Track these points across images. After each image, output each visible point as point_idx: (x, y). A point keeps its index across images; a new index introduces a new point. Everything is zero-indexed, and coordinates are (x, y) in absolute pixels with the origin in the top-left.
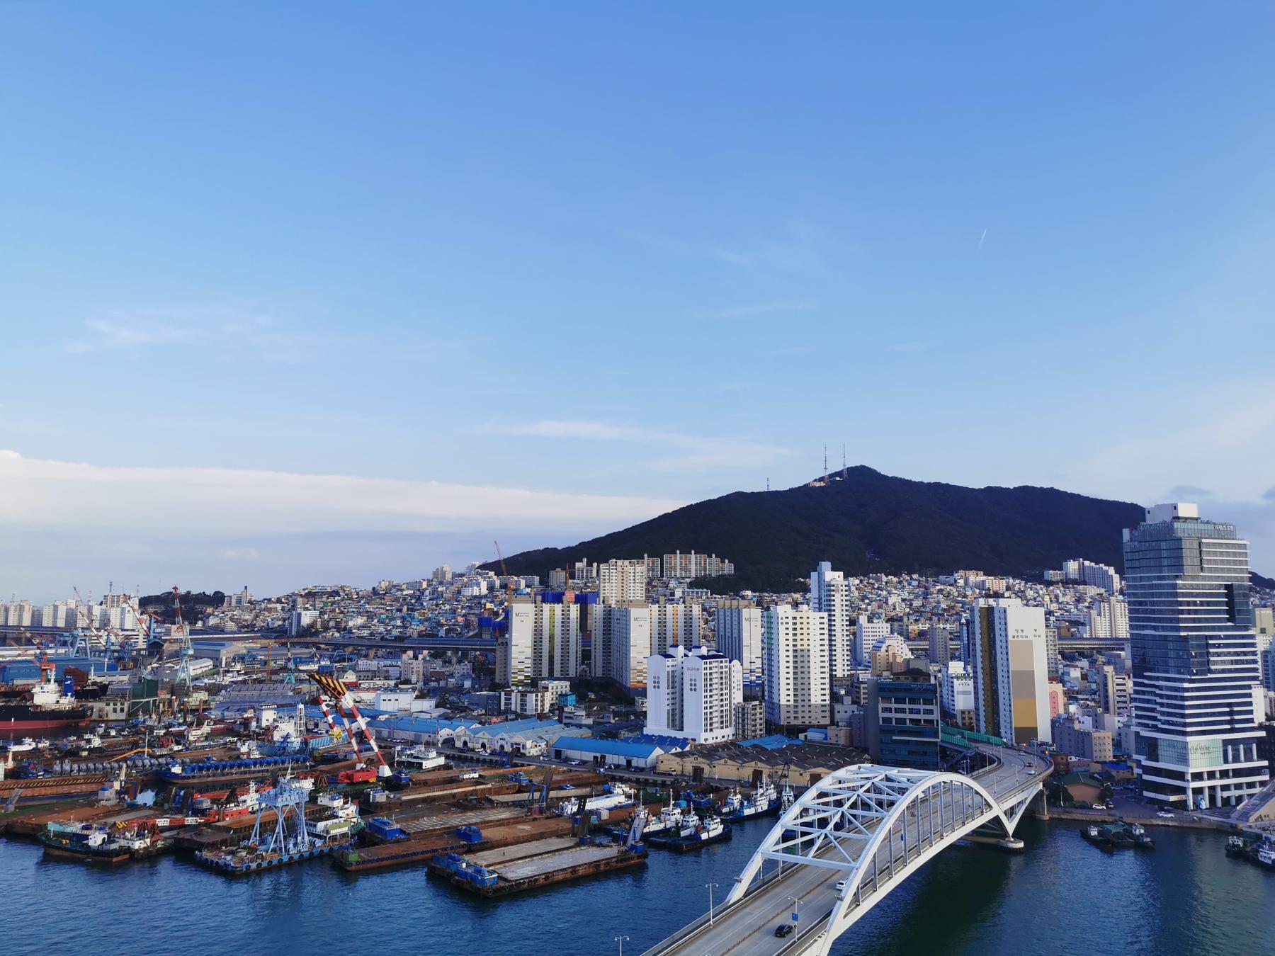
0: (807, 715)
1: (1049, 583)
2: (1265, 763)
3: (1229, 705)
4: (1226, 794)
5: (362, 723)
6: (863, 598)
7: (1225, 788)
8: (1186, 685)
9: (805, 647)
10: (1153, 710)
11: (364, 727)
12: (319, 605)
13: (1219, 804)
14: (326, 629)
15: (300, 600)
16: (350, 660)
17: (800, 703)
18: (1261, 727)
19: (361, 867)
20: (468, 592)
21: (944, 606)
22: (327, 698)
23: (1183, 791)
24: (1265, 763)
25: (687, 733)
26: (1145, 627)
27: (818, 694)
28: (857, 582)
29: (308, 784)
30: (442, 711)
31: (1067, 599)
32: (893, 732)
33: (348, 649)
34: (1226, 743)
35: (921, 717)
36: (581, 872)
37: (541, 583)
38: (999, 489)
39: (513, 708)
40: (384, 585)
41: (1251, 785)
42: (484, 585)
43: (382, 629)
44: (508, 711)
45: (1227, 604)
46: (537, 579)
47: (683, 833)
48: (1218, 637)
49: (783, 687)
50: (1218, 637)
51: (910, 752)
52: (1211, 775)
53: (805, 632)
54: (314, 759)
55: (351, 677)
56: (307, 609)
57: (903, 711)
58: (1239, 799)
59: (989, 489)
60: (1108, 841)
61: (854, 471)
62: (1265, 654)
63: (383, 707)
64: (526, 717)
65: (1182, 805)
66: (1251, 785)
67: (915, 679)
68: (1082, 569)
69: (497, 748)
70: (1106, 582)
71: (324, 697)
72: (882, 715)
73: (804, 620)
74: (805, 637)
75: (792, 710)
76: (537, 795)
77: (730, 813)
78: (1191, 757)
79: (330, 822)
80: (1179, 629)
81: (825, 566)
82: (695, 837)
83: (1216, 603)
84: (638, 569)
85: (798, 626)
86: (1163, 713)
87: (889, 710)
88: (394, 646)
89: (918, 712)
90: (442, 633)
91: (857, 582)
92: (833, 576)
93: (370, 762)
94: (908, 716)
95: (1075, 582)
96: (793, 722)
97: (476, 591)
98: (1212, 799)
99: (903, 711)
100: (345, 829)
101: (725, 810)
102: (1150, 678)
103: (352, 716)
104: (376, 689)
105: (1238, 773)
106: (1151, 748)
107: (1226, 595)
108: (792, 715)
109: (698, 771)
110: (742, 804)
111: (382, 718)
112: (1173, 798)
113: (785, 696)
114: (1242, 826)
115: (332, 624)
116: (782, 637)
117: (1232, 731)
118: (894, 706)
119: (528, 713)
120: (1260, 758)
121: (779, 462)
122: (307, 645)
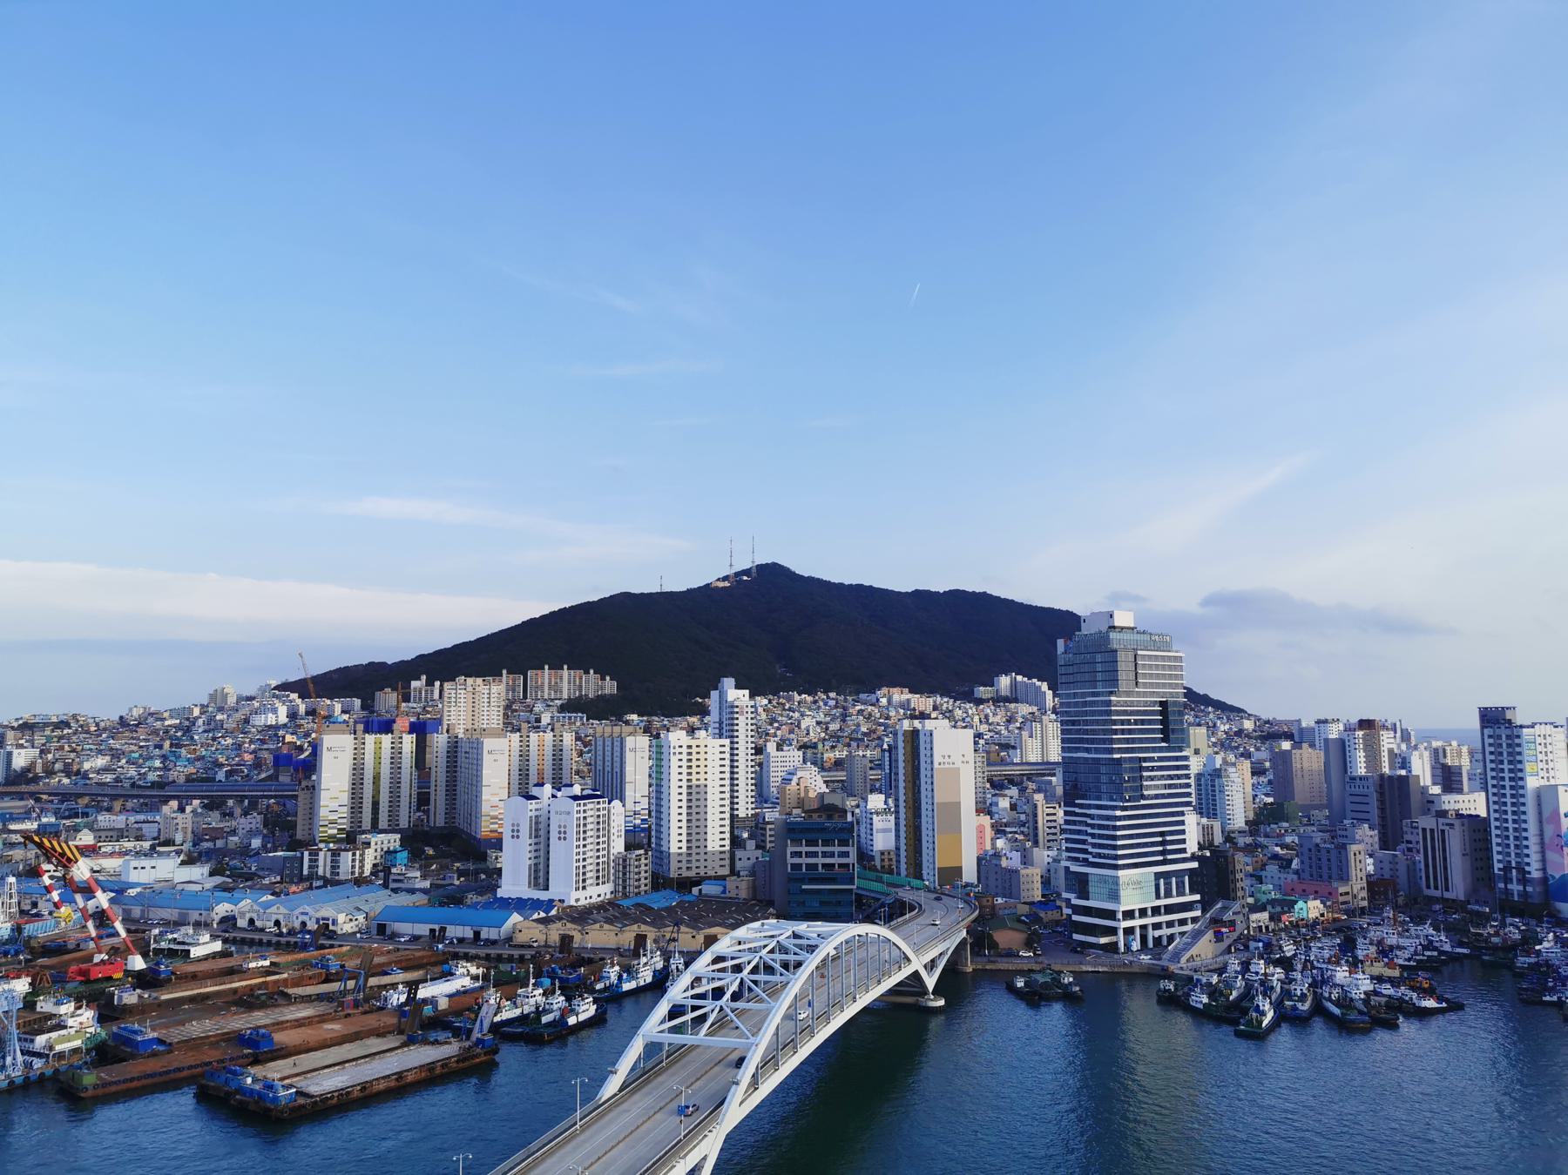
0: (702, 864)
1: (979, 702)
2: (1197, 897)
3: (1162, 834)
4: (1157, 933)
5: (102, 899)
6: (772, 721)
7: (1157, 926)
8: (1118, 813)
9: (702, 782)
10: (1084, 842)
11: (105, 905)
12: (39, 740)
13: (1151, 944)
14: (50, 772)
15: (10, 735)
16: (85, 815)
17: (694, 851)
18: (1193, 858)
19: (100, 1092)
20: (260, 720)
21: (864, 729)
22: (51, 867)
23: (1113, 931)
24: (1197, 897)
25: (553, 893)
26: (1077, 750)
27: (717, 839)
28: (765, 702)
29: (21, 986)
30: (218, 880)
31: (997, 719)
32: (803, 880)
33: (82, 800)
34: (1158, 876)
35: (836, 860)
36: (410, 1078)
37: (363, 708)
38: (928, 593)
39: (321, 872)
40: (135, 713)
41: (1183, 922)
42: (283, 712)
43: (132, 772)
44: (313, 876)
45: (1162, 722)
46: (357, 702)
47: (544, 1019)
48: (1151, 759)
49: (674, 831)
50: (1151, 759)
51: (822, 903)
52: (1143, 912)
53: (702, 763)
54: (32, 951)
55: (86, 838)
56: (22, 746)
57: (815, 855)
58: (1171, 938)
59: (917, 593)
60: (1034, 993)
62: (1199, 776)
63: (134, 877)
64: (339, 883)
65: (1113, 947)
66: (1183, 922)
67: (830, 817)
68: (1014, 684)
69: (297, 925)
70: (1038, 700)
71: (45, 867)
72: (790, 861)
73: (702, 750)
74: (702, 769)
75: (684, 858)
76: (351, 984)
77: (606, 989)
78: (1122, 893)
79: (54, 1035)
80: (1111, 751)
81: (728, 683)
82: (560, 1022)
83: (1150, 722)
84: (495, 689)
85: (694, 757)
86: (1094, 845)
87: (799, 854)
88: (150, 796)
89: (832, 855)
90: (221, 776)
91: (765, 702)
92: (737, 696)
93: (114, 951)
94: (820, 861)
95: (1007, 700)
96: (685, 874)
97: (271, 719)
98: (1144, 938)
99: (815, 855)
100: (77, 1043)
101: (599, 986)
102: (1081, 806)
103: (88, 892)
104: (122, 854)
105: (1170, 909)
106: (1080, 884)
107: (1161, 713)
108: (684, 865)
109: (566, 940)
110: (620, 978)
111: (132, 892)
112: (1103, 940)
113: (676, 842)
114: (1173, 968)
115: (58, 766)
116: (674, 770)
117: (1164, 862)
118: (804, 849)
119: (342, 877)
120: (1192, 891)
121: (676, 555)
122: (21, 796)
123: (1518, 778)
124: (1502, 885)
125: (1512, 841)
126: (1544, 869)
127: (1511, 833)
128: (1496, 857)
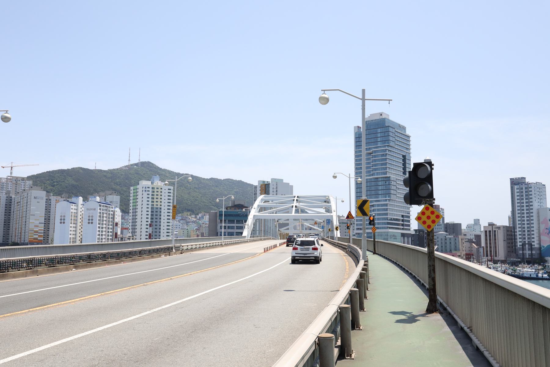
9: (159, 206)
53: (159, 197)
59: (211, 179)
61: (143, 164)
74: (159, 200)
99: (233, 228)
123: (529, 206)
124: (521, 252)
125: (526, 233)
126: (540, 244)
127: (526, 230)
128: (518, 240)
